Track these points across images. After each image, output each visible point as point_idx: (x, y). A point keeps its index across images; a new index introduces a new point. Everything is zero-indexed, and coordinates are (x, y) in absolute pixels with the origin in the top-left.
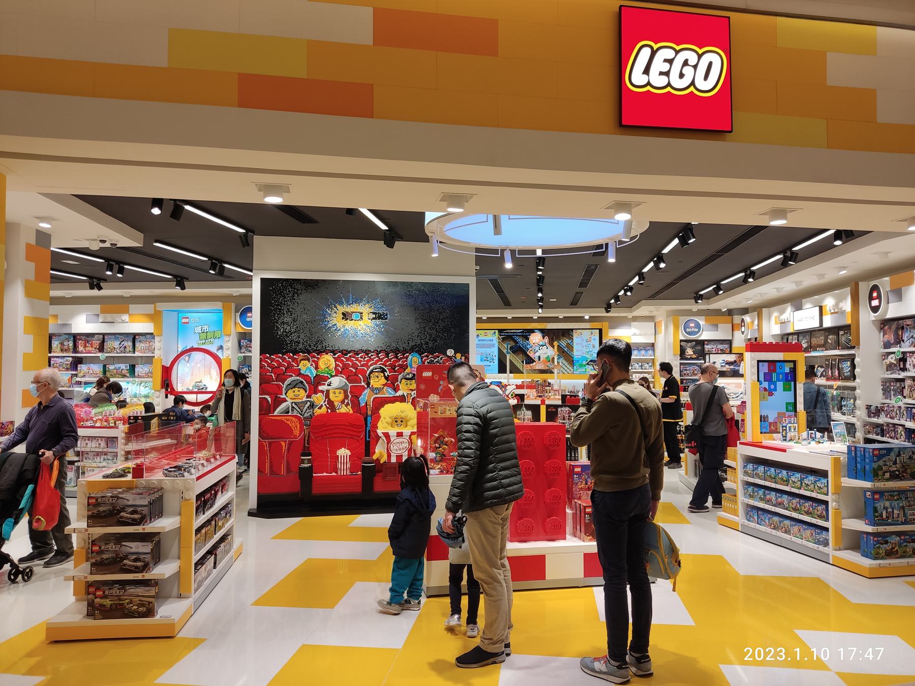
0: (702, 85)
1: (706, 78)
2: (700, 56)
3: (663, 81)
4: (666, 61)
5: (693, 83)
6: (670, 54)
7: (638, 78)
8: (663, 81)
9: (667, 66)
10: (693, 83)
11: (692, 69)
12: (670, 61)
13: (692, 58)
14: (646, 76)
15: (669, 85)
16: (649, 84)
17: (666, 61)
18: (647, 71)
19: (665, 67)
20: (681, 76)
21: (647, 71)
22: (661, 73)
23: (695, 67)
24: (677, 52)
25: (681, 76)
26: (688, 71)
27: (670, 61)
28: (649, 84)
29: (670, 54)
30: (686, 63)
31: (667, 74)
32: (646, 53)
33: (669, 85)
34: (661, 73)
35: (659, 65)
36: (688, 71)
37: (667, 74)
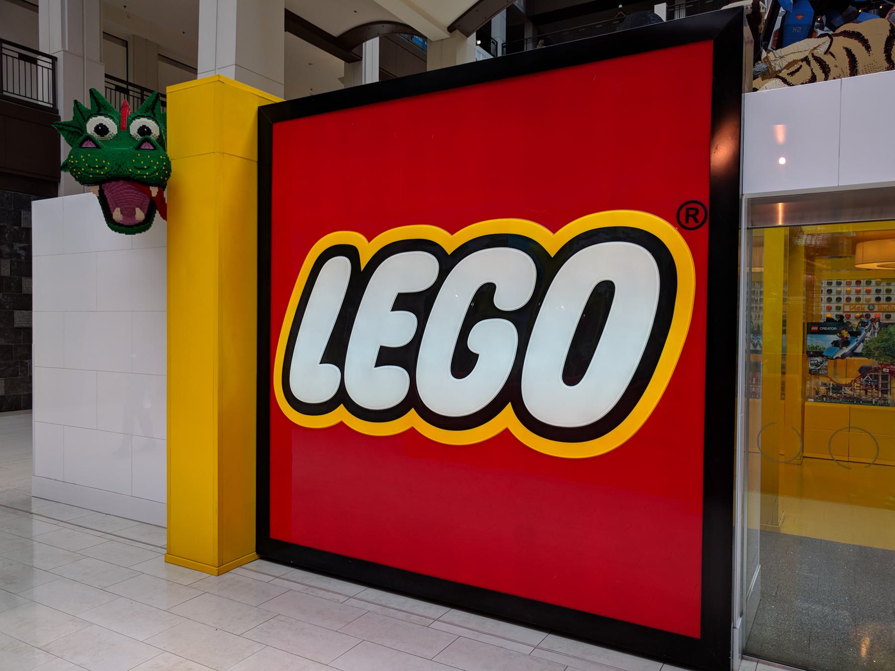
0: (551, 398)
1: (574, 371)
2: (547, 267)
4: (403, 302)
5: (511, 393)
6: (413, 271)
7: (311, 379)
9: (408, 321)
10: (511, 393)
11: (507, 331)
12: (418, 304)
13: (510, 275)
14: (332, 370)
15: (412, 400)
16: (342, 397)
17: (403, 302)
18: (336, 353)
19: (399, 329)
20: (463, 362)
21: (336, 353)
22: (386, 357)
23: (524, 320)
24: (447, 262)
25: (463, 362)
26: (494, 341)
27: (418, 304)
28: (342, 397)
29: (413, 271)
30: (483, 305)
31: (404, 357)
32: (336, 276)
33: (412, 400)
34: (386, 357)
35: (381, 324)
36: (494, 341)
37: (404, 357)
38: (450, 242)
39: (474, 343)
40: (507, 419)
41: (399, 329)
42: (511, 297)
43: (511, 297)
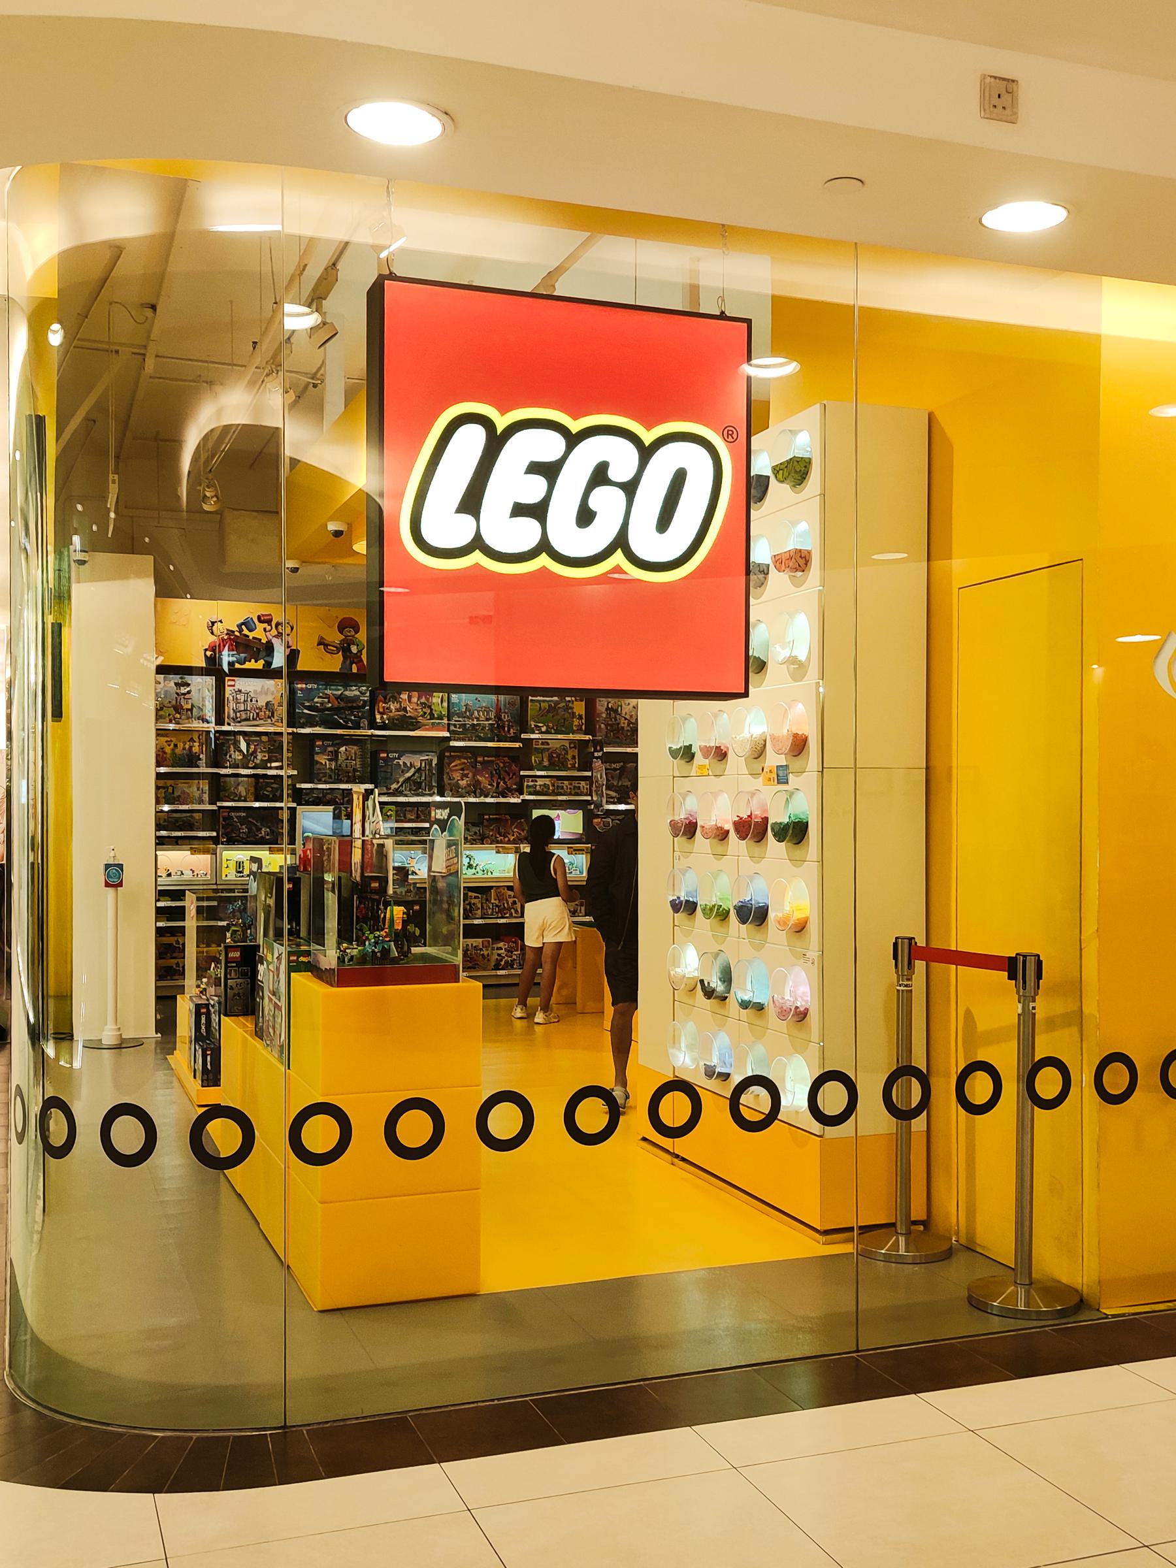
0: (649, 543)
1: (664, 521)
2: (646, 453)
3: (526, 534)
4: (535, 468)
5: (621, 542)
6: (548, 446)
8: (526, 534)
10: (621, 542)
12: (549, 471)
13: (622, 459)
14: (469, 519)
15: (544, 546)
16: (477, 543)
17: (535, 468)
18: (471, 503)
19: (533, 489)
20: (585, 517)
21: (471, 503)
22: (519, 510)
23: (630, 488)
24: (573, 440)
25: (585, 517)
26: (607, 501)
27: (549, 471)
28: (477, 543)
29: (548, 446)
30: (600, 476)
31: (538, 511)
32: (471, 439)
33: (544, 546)
34: (519, 510)
35: (511, 481)
36: (607, 501)
37: (538, 511)
39: (593, 504)
40: (618, 558)
41: (533, 489)
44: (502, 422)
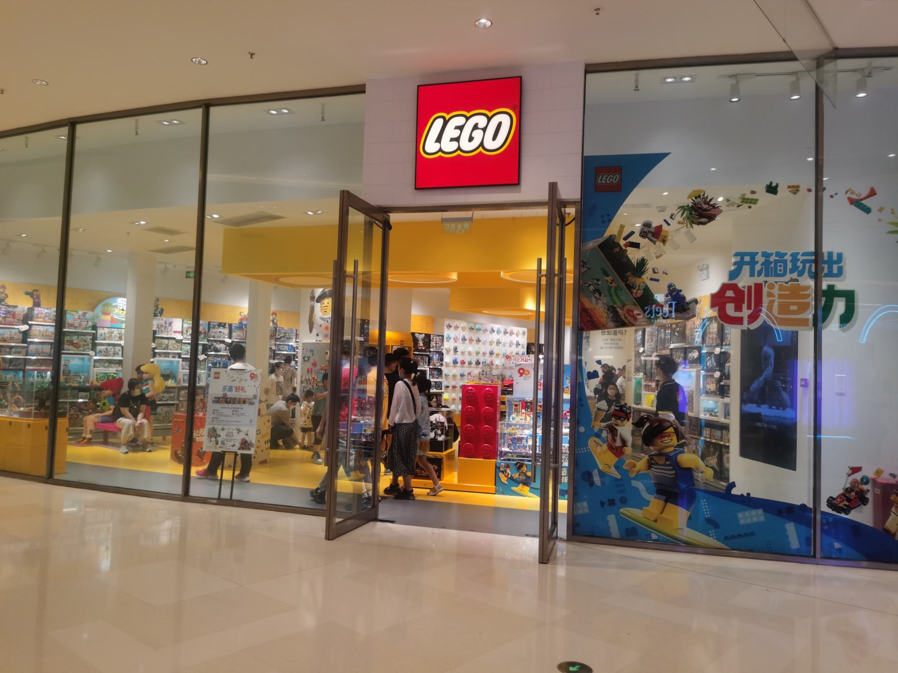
1: (494, 138)
2: (489, 119)
3: (455, 145)
4: (456, 128)
5: (482, 144)
6: (460, 121)
7: (431, 146)
8: (455, 145)
9: (458, 131)
10: (482, 144)
11: (481, 132)
12: (461, 128)
15: (459, 148)
16: (440, 150)
17: (456, 128)
18: (439, 140)
20: (471, 139)
21: (439, 140)
22: (452, 140)
23: (484, 130)
24: (467, 119)
25: (471, 139)
26: (478, 135)
27: (461, 128)
28: (440, 150)
29: (460, 121)
30: (476, 127)
31: (457, 139)
32: (439, 123)
33: (459, 148)
34: (452, 140)
35: (451, 132)
36: (478, 135)
37: (457, 139)
38: (468, 115)
40: (481, 149)
42: (481, 126)
43: (481, 126)
44: (447, 117)
